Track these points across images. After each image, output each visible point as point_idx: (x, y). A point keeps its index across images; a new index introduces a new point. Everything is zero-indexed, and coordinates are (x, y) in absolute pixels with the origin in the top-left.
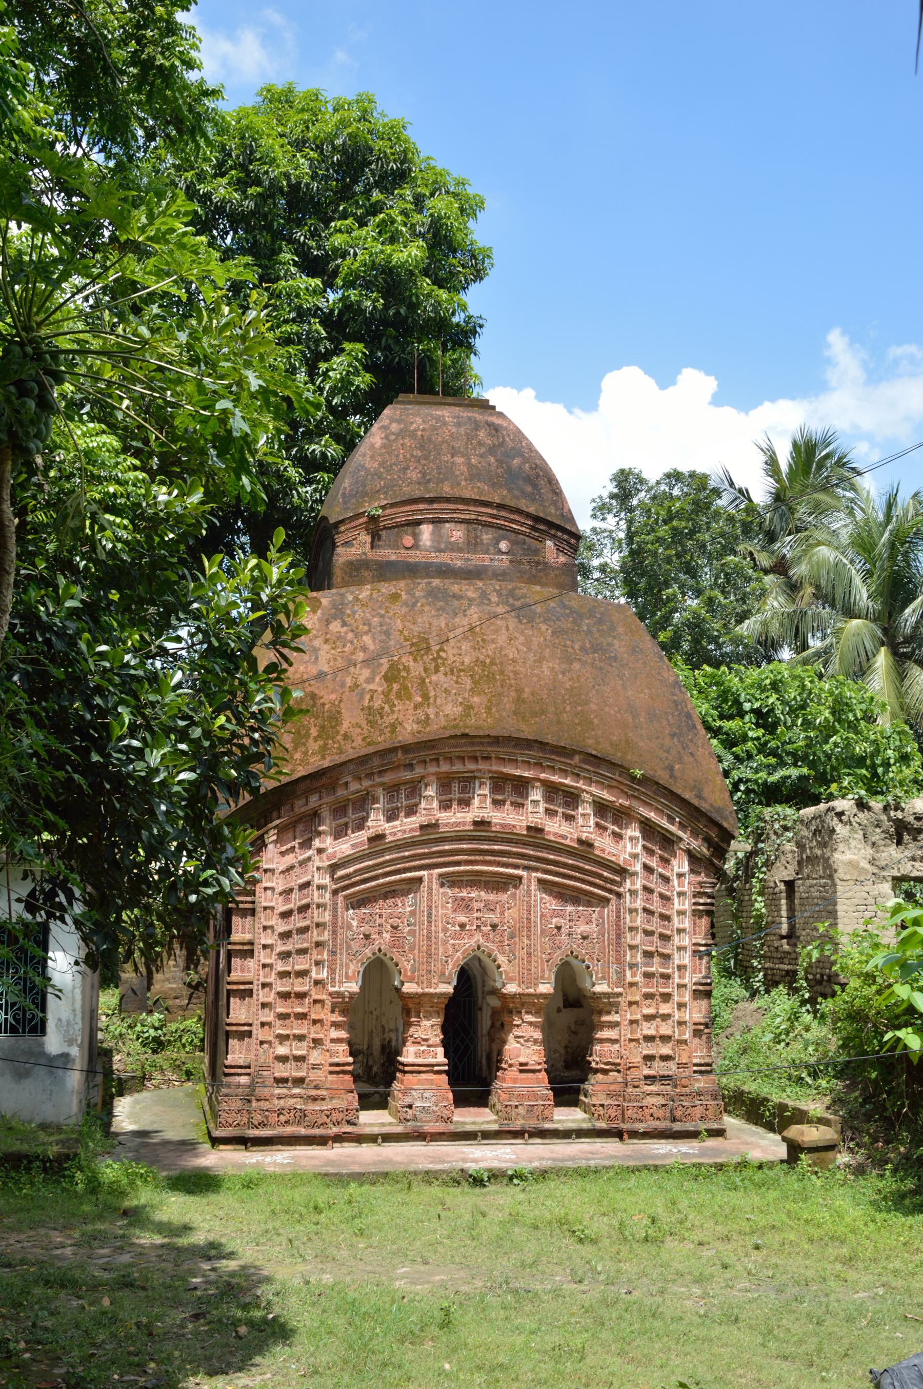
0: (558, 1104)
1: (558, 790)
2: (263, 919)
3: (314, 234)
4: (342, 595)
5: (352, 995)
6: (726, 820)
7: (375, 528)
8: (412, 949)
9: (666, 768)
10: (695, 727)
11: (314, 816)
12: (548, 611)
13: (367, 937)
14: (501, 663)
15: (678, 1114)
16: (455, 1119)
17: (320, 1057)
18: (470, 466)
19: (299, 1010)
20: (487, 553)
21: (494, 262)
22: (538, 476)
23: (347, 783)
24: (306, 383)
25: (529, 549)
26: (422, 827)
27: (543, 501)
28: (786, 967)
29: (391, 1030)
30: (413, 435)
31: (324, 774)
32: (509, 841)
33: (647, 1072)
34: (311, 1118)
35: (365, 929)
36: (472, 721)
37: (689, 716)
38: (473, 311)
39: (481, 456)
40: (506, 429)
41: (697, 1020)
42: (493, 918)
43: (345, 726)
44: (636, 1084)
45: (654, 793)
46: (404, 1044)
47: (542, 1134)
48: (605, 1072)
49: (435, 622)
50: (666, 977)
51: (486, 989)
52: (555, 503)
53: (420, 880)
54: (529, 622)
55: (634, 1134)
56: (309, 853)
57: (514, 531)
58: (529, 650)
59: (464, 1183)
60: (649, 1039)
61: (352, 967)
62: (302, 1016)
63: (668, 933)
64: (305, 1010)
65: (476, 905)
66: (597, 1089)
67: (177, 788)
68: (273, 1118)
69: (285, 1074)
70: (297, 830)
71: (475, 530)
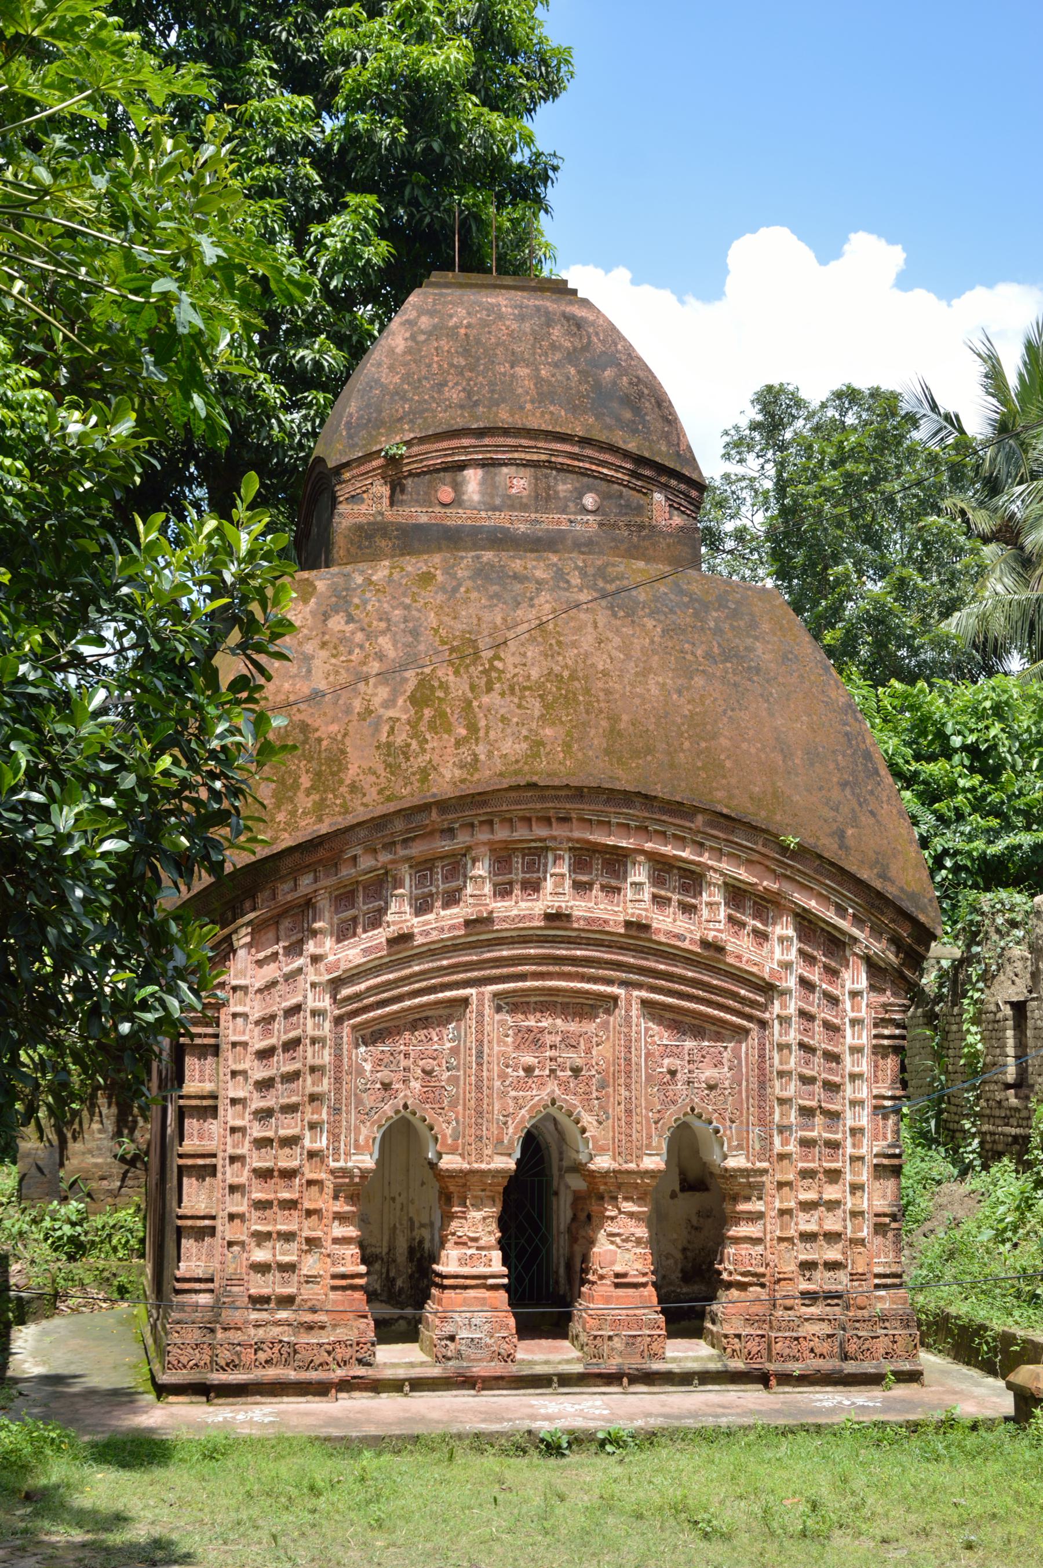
0: (672, 1334)
1: (673, 867)
2: (231, 1060)
3: (302, 29)
4: (347, 576)
5: (364, 1174)
6: (923, 910)
7: (395, 474)
8: (453, 1105)
9: (832, 834)
10: (876, 772)
11: (307, 906)
12: (656, 599)
13: (386, 1086)
14: (586, 678)
15: (852, 1348)
16: (519, 1356)
17: (318, 1265)
18: (538, 380)
19: (286, 1195)
20: (564, 511)
21: (575, 69)
22: (641, 395)
23: (355, 858)
24: (290, 256)
25: (627, 506)
26: (468, 923)
27: (649, 432)
28: (1013, 1131)
29: (422, 1226)
30: (452, 333)
31: (321, 844)
32: (599, 944)
33: (804, 1286)
34: (303, 1355)
35: (384, 1075)
36: (543, 765)
37: (868, 756)
38: (542, 145)
39: (556, 365)
40: (593, 324)
41: (880, 1210)
42: (576, 1058)
43: (352, 772)
44: (789, 1302)
45: (816, 871)
46: (442, 1245)
47: (649, 1378)
48: (743, 1286)
49: (487, 616)
50: (834, 1145)
51: (565, 1164)
52: (666, 436)
53: (465, 1001)
54: (627, 615)
55: (786, 1379)
56: (300, 962)
57: (606, 479)
58: (628, 657)
59: (532, 1451)
60: (808, 1237)
61: (364, 1131)
62: (291, 1205)
63: (837, 1079)
64: (295, 1196)
65: (549, 1039)
66: (730, 1310)
67: (99, 864)
68: (248, 1355)
69: (266, 1291)
70: (282, 927)
71: (546, 477)
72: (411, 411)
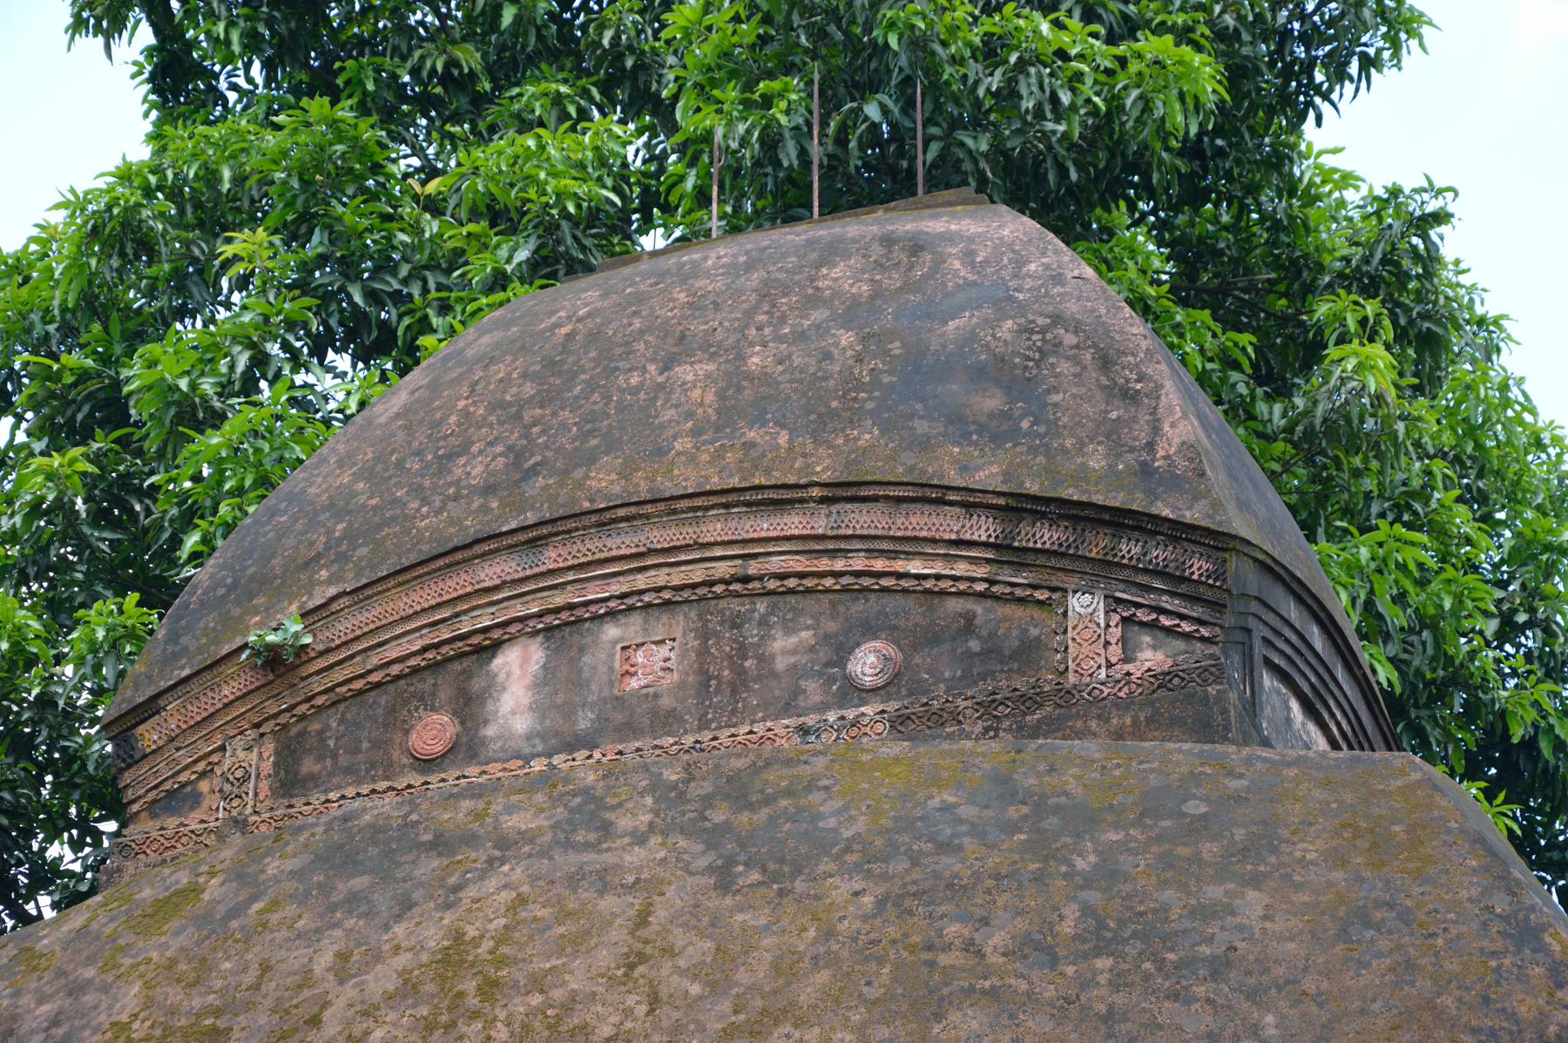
20: (788, 709)
25: (992, 651)
27: (1054, 428)
58: (715, 989)
71: (736, 623)
72: (348, 535)
